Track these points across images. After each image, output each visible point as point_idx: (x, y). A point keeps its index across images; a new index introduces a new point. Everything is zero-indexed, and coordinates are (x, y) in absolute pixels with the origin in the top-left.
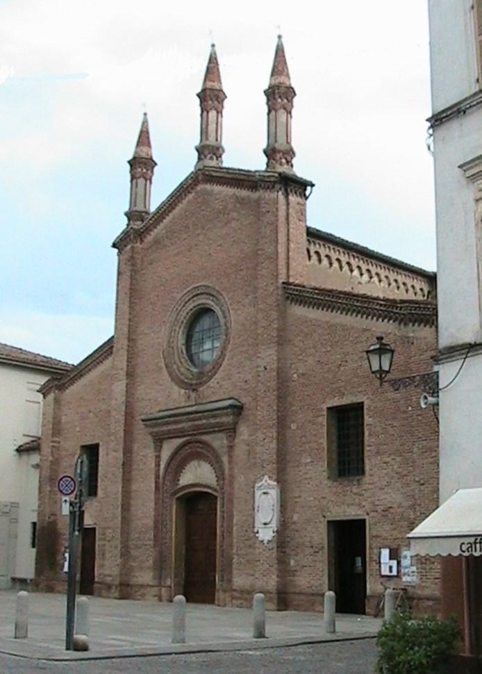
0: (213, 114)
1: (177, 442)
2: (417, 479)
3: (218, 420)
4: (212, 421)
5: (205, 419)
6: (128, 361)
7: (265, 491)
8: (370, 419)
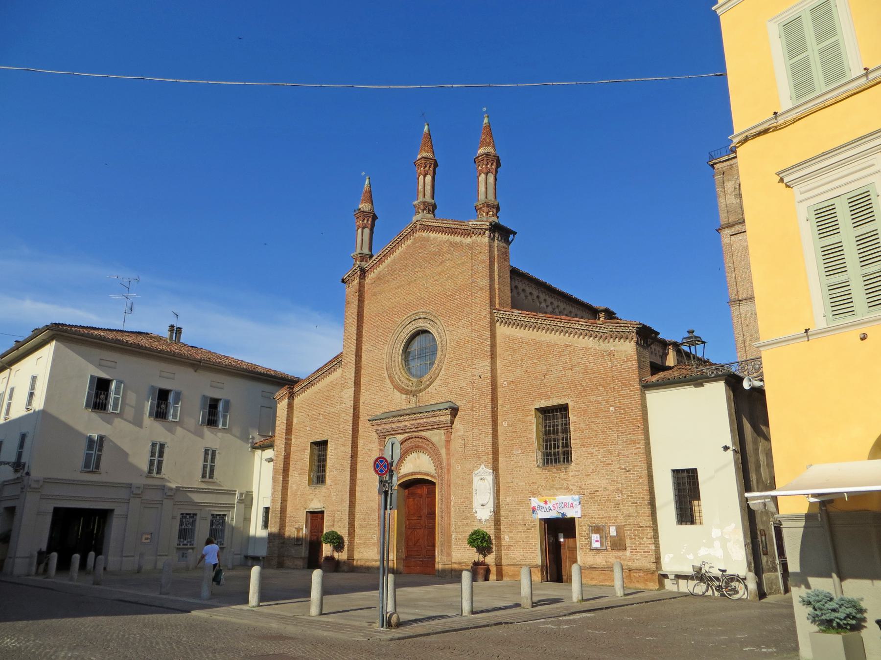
2: (623, 467)
4: (432, 420)
7: (482, 477)
8: (575, 417)
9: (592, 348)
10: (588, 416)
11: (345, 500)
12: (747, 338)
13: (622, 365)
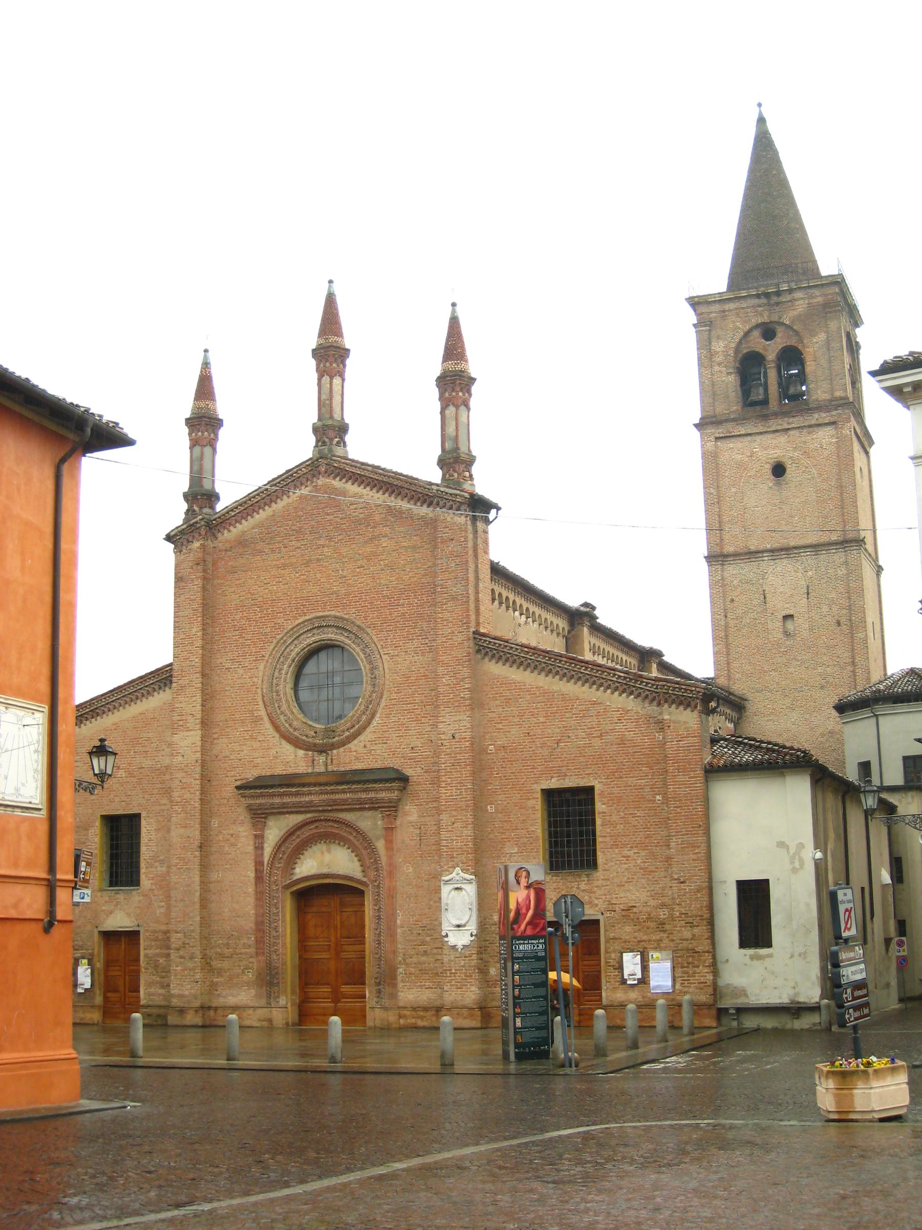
0: (337, 381)
1: (294, 820)
2: (676, 877)
3: (372, 795)
4: (363, 796)
5: (350, 792)
6: (202, 705)
7: (456, 886)
8: (603, 806)
9: (632, 710)
10: (624, 805)
11: (191, 914)
12: (732, 623)
13: (680, 741)
